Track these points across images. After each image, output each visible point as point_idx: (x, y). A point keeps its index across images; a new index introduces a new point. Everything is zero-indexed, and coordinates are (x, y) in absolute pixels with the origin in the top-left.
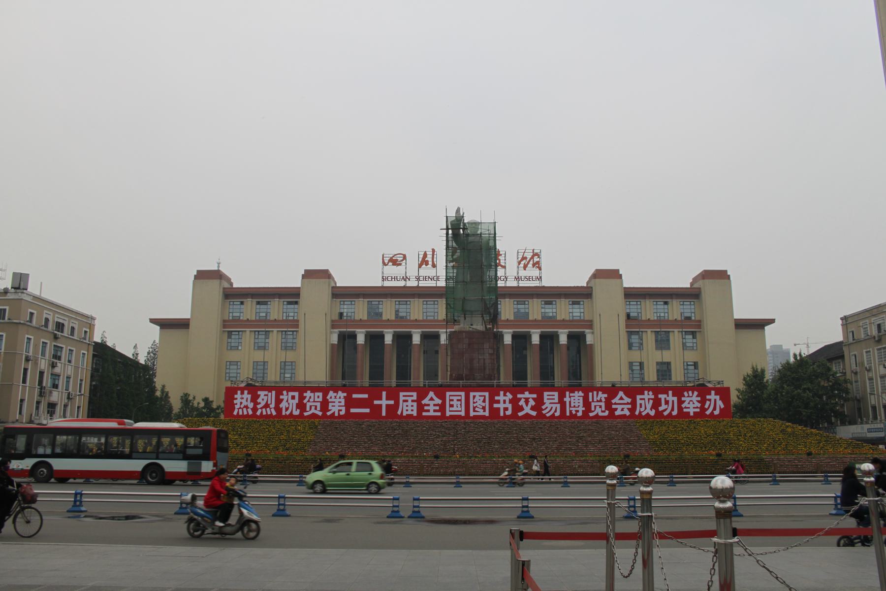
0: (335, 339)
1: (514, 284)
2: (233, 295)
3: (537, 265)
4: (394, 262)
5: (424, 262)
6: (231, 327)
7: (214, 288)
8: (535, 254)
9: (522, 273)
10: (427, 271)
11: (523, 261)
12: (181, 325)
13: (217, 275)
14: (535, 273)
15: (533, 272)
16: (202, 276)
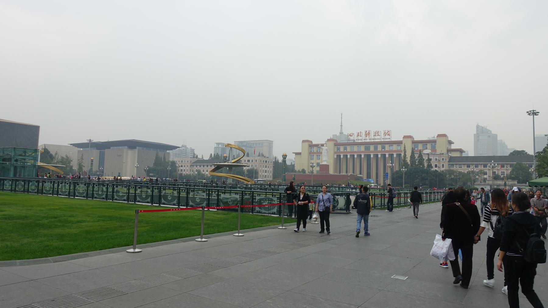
0: (335, 157)
1: (383, 140)
2: (311, 146)
3: (389, 135)
4: (351, 136)
5: (358, 135)
6: (311, 153)
7: (307, 144)
8: (388, 132)
9: (386, 137)
10: (360, 138)
11: (385, 134)
12: (300, 154)
13: (308, 141)
14: (388, 137)
15: (387, 137)
16: (304, 141)
